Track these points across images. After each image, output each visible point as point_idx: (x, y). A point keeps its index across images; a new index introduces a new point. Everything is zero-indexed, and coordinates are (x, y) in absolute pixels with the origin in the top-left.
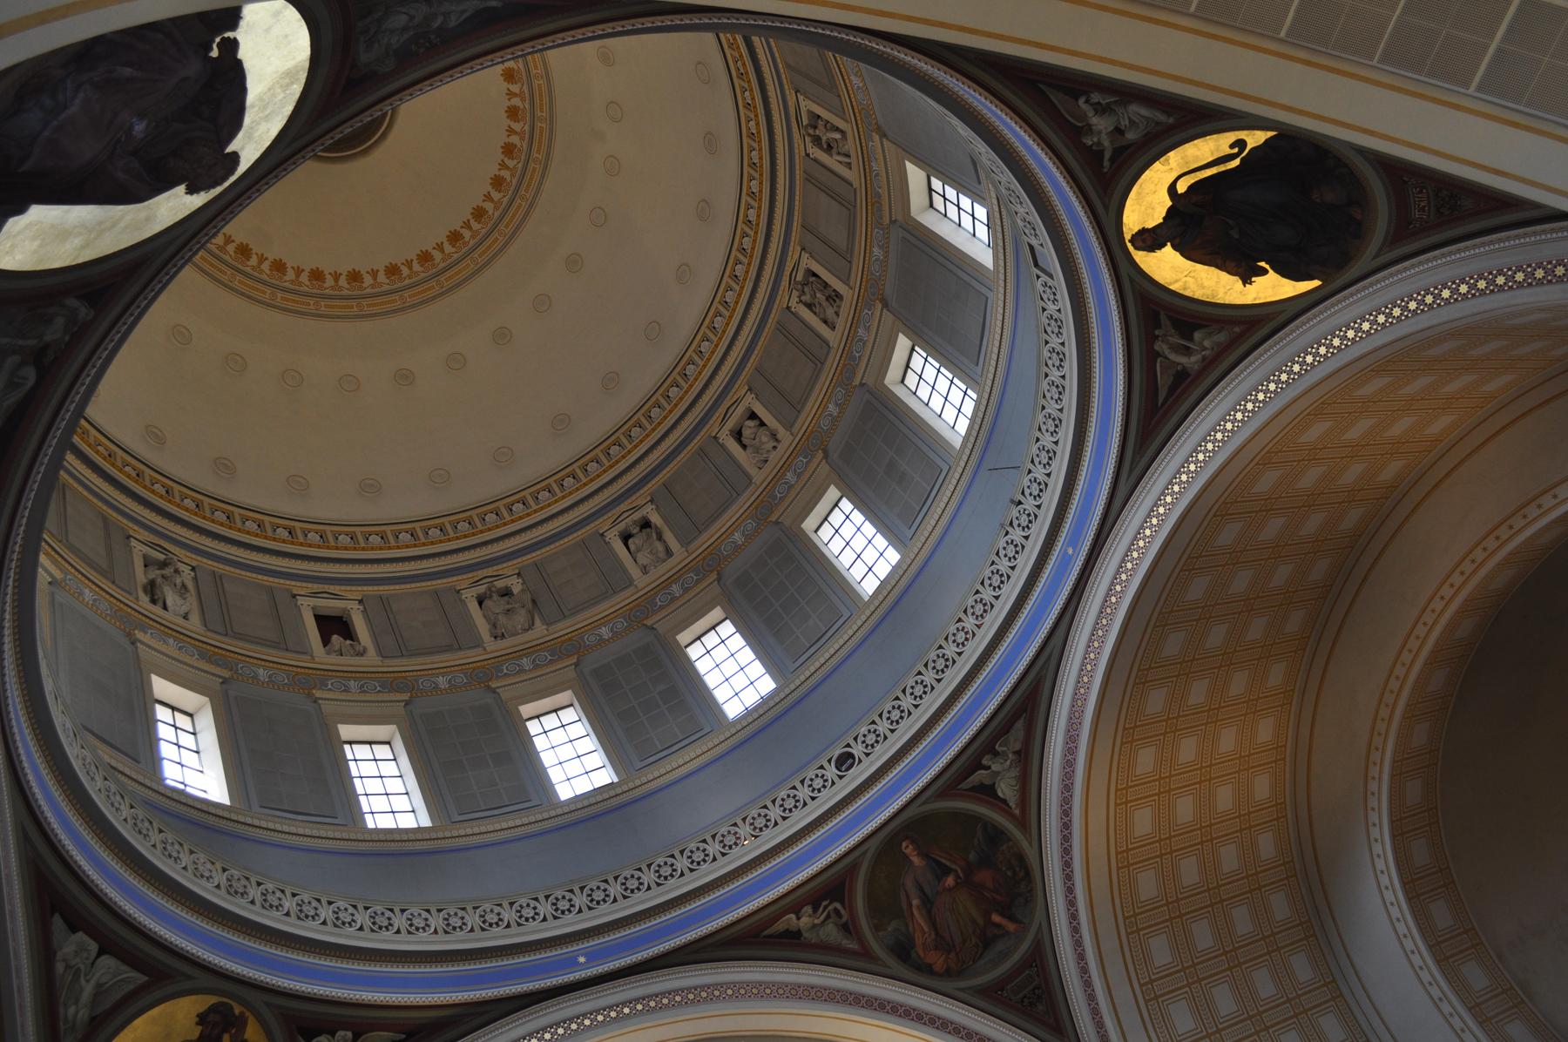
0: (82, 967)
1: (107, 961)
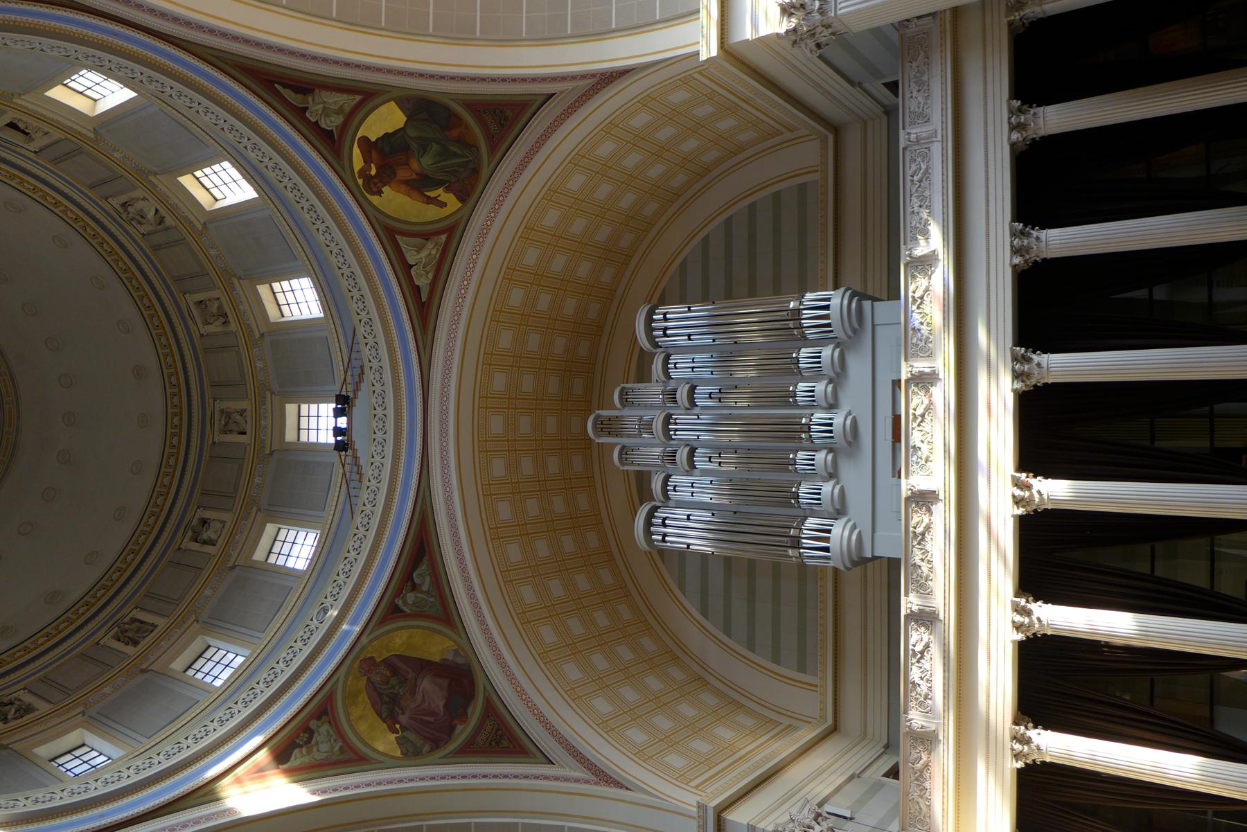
1: (411, 261)
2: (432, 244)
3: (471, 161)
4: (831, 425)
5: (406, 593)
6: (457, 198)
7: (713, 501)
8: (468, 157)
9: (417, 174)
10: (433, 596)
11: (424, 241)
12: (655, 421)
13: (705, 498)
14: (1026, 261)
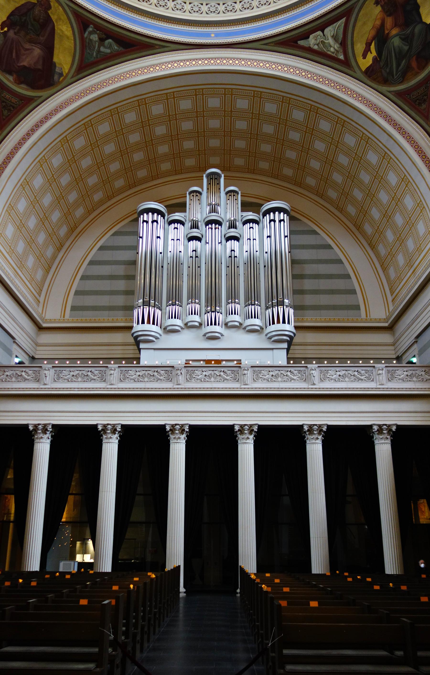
0: (322, 40)
1: (327, 31)
2: (338, 48)
3: (393, 78)
4: (215, 324)
5: (96, 33)
6: (368, 67)
7: (169, 253)
8: (396, 75)
9: (388, 34)
10: (97, 55)
11: (340, 41)
12: (217, 214)
13: (170, 248)
14: (305, 432)
